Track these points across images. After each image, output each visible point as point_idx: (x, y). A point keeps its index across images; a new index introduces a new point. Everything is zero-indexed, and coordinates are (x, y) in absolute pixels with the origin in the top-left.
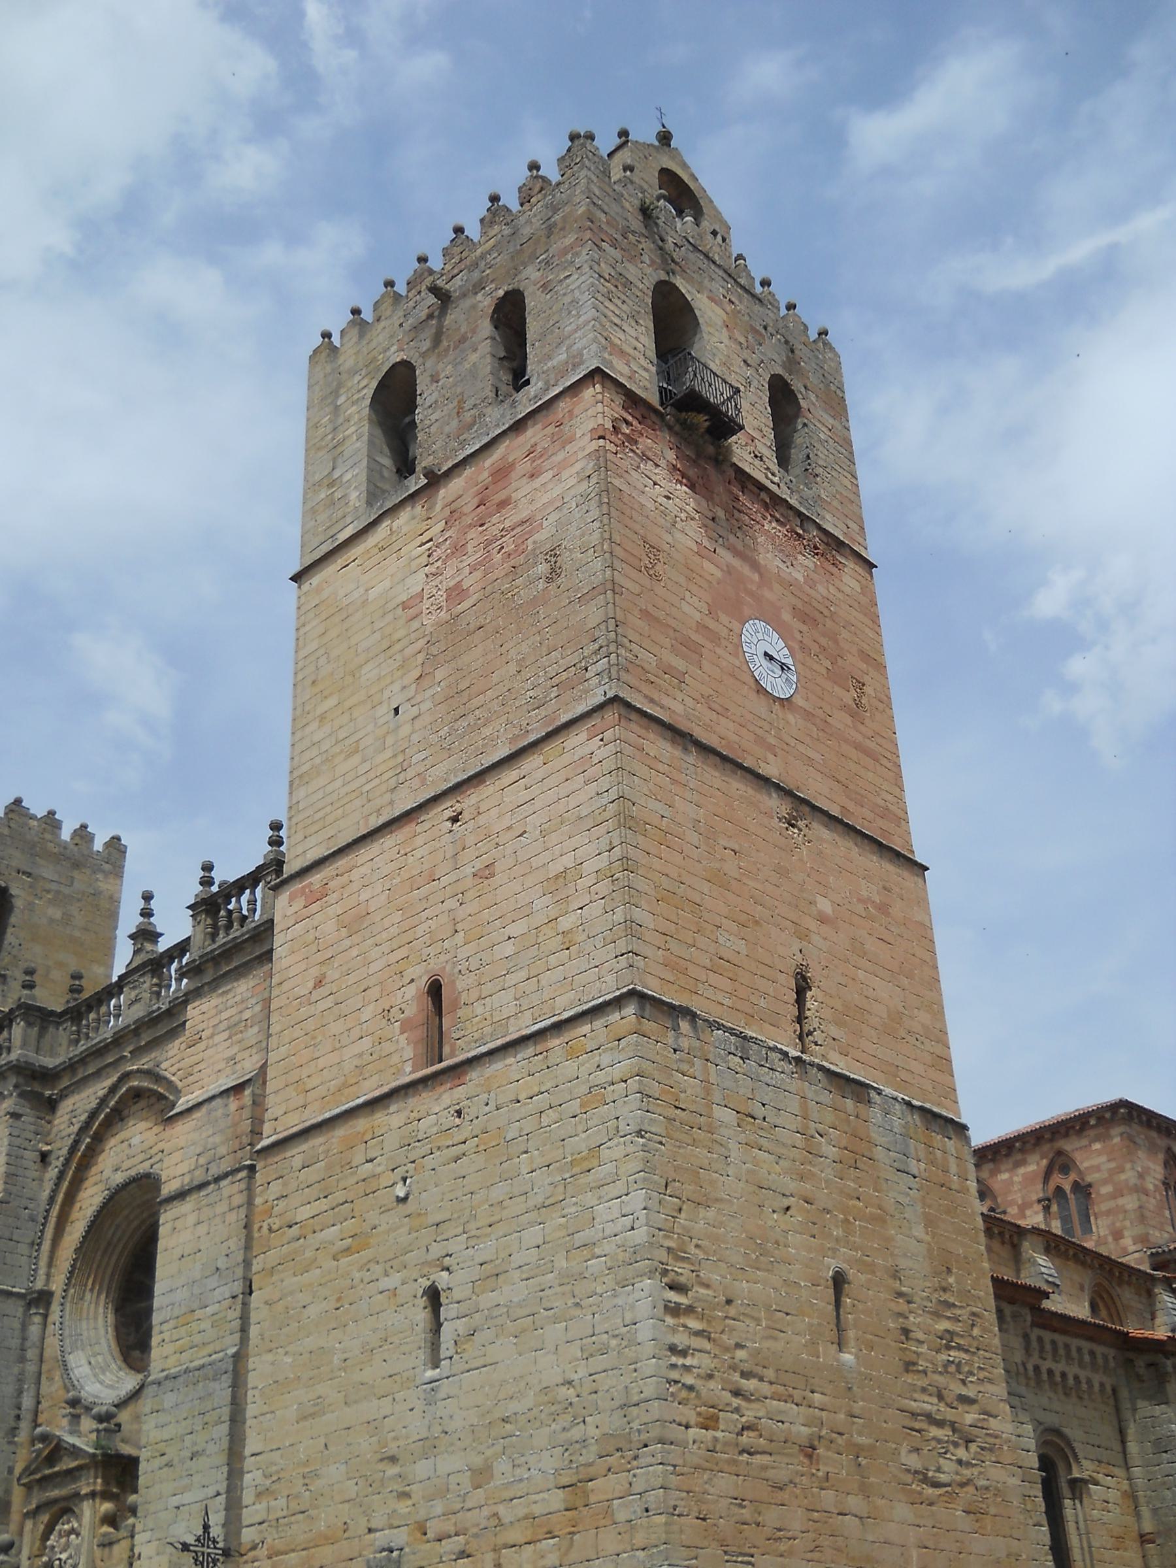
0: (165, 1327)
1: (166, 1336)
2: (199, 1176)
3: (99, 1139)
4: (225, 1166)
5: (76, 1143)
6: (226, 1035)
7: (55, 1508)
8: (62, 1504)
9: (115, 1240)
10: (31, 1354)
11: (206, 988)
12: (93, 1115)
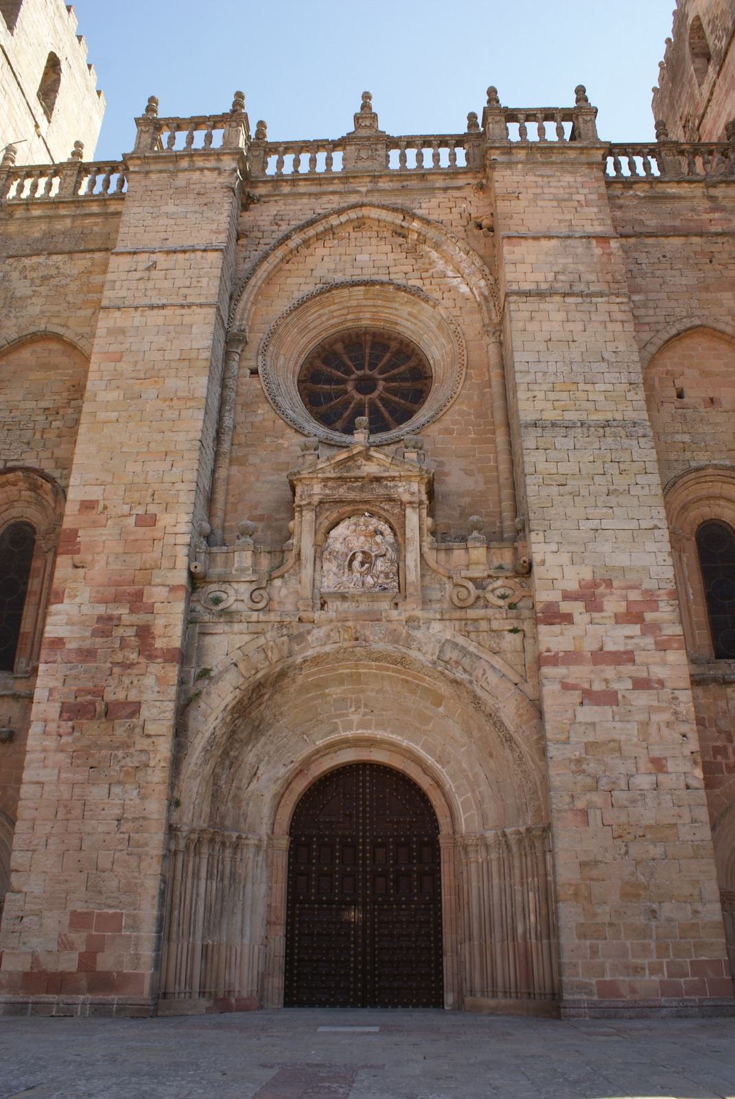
0: (535, 387)
1: (540, 395)
3: (306, 243)
4: (593, 288)
5: (287, 237)
6: (555, 204)
9: (312, 326)
10: (231, 382)
11: (520, 166)
12: (311, 223)
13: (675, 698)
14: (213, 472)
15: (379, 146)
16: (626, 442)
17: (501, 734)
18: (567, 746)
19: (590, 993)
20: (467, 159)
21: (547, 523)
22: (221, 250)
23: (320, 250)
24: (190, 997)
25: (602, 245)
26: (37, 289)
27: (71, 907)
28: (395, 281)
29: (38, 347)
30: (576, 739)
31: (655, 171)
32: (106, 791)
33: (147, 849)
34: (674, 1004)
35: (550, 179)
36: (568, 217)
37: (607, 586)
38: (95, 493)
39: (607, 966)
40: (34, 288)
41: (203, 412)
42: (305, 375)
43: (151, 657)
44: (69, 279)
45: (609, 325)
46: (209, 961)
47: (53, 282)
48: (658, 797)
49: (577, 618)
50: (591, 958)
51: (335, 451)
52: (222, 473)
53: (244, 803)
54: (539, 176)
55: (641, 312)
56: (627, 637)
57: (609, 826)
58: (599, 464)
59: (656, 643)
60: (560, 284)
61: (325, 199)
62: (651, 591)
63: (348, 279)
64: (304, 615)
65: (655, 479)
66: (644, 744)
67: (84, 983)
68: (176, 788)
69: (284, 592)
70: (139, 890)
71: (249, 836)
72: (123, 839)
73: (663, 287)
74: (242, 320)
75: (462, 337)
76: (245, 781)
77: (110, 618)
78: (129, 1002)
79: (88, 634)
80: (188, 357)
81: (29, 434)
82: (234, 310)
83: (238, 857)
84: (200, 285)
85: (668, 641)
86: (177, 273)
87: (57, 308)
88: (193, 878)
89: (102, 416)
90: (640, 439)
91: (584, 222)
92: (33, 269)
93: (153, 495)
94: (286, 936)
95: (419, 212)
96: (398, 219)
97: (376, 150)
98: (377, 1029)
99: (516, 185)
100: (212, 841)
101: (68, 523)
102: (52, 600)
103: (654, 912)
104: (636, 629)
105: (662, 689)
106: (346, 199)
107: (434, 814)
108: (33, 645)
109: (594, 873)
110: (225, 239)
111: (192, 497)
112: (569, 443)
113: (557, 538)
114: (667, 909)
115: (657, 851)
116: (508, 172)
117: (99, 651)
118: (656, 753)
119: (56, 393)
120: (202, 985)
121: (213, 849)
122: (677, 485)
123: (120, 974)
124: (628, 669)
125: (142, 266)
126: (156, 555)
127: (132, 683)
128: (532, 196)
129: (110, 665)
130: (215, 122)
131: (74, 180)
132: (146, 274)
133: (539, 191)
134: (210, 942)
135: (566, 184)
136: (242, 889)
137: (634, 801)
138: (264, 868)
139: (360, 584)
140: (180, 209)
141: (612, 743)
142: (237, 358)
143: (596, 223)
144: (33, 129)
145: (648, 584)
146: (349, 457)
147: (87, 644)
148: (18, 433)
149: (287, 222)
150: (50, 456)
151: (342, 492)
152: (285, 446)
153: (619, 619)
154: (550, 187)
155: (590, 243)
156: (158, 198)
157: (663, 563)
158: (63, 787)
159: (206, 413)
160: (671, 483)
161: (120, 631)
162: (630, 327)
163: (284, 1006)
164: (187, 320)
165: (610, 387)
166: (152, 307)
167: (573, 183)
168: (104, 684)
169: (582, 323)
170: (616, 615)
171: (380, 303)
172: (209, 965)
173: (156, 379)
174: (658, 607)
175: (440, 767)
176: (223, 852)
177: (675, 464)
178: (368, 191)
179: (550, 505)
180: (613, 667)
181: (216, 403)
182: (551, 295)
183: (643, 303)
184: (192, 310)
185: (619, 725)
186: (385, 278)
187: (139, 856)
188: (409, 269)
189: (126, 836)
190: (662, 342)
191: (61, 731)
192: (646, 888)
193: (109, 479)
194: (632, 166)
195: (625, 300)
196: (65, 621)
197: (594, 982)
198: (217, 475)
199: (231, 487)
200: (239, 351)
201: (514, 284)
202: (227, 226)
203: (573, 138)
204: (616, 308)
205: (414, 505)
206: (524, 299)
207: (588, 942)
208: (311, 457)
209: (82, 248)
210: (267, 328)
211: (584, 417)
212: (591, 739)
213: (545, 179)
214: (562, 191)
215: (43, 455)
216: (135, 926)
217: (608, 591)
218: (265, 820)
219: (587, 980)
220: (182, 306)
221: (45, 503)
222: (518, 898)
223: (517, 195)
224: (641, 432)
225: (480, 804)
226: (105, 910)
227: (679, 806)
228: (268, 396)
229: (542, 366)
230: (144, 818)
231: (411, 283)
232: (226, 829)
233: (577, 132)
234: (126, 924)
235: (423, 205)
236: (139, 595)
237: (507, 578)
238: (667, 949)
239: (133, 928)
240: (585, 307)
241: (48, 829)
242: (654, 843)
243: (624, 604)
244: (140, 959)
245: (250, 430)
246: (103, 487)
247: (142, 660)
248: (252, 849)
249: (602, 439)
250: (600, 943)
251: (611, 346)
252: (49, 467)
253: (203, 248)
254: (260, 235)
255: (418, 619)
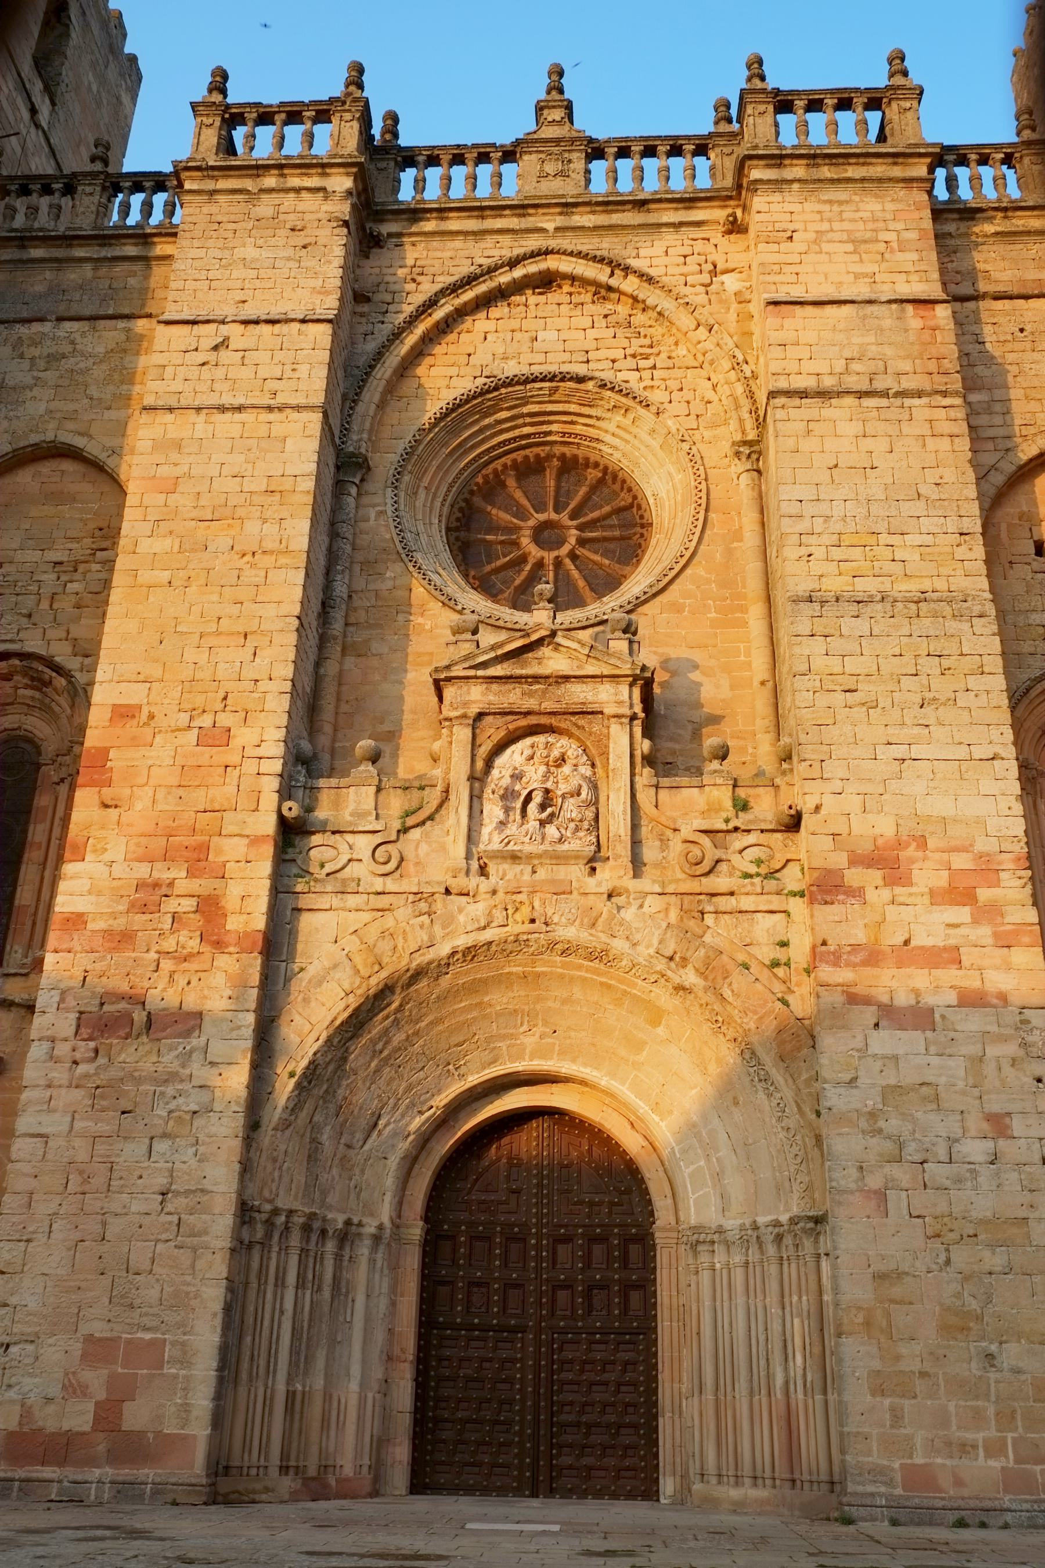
0: (813, 540)
1: (819, 553)
2: (853, 382)
3: (461, 313)
4: (908, 383)
5: (432, 303)
6: (850, 247)
7: (523, 722)
8: (544, 720)
10: (345, 529)
11: (796, 186)
12: (469, 281)
13: (1028, 1022)
14: (318, 665)
15: (574, 156)
16: (952, 626)
17: (752, 1070)
18: (855, 1091)
19: (890, 1483)
20: (713, 176)
21: (825, 748)
22: (329, 321)
23: (480, 323)
24: (266, 1474)
25: (922, 313)
26: (41, 375)
27: (84, 1329)
28: (597, 374)
29: (46, 468)
30: (869, 1081)
31: (1013, 192)
32: (144, 1148)
33: (205, 1238)
34: (1025, 1506)
35: (843, 208)
36: (873, 268)
37: (918, 847)
38: (134, 694)
39: (919, 1441)
40: (35, 374)
41: (302, 573)
42: (458, 520)
43: (219, 945)
44: (91, 360)
45: (929, 441)
46: (297, 1416)
47: (69, 363)
48: (997, 1174)
49: (871, 895)
50: (892, 1426)
51: (503, 636)
52: (331, 668)
53: (357, 1171)
54: (825, 202)
55: (983, 420)
56: (949, 925)
57: (918, 1217)
58: (908, 658)
59: (996, 935)
60: (855, 378)
61: (490, 241)
62: (988, 855)
63: (525, 370)
64: (454, 884)
65: (999, 682)
66: (976, 1092)
67: (101, 1448)
68: (254, 1145)
69: (424, 848)
70: (193, 1303)
71: (365, 1220)
72: (170, 1223)
73: (1018, 379)
74: (361, 432)
75: (699, 462)
76: (359, 1136)
77: (156, 885)
78: (173, 1480)
79: (122, 907)
80: (281, 488)
81: (30, 601)
82: (350, 416)
83: (347, 1253)
84: (296, 375)
85: (1016, 933)
86: (263, 357)
87: (71, 407)
88: (276, 1285)
89: (146, 576)
90: (975, 621)
91: (896, 277)
92: (34, 343)
93: (225, 698)
94: (416, 1380)
95: (634, 263)
96: (601, 273)
97: (570, 161)
98: (556, 1528)
99: (788, 217)
100: (307, 1228)
101: (92, 739)
102: (67, 855)
103: (990, 1356)
104: (963, 914)
105: (1005, 1007)
106: (524, 243)
107: (646, 1191)
108: (34, 924)
109: (897, 1291)
110: (336, 304)
111: (285, 702)
112: (862, 626)
113: (842, 773)
114: (1012, 1354)
115: (996, 1260)
116: (777, 197)
117: (140, 934)
118: (995, 1106)
119: (72, 539)
120: (285, 1455)
121: (308, 1241)
122: (1033, 693)
123: (158, 1434)
124: (949, 976)
125: (207, 343)
126: (232, 789)
127: (189, 983)
128: (813, 235)
129: (156, 956)
130: (323, 113)
131: (96, 201)
132: (212, 357)
133: (825, 226)
134: (299, 1387)
135: (869, 214)
136: (350, 1304)
137: (959, 1180)
138: (386, 1271)
139: (539, 838)
140: (265, 253)
141: (924, 1089)
142: (354, 491)
143: (914, 277)
144: (26, 115)
145: (982, 845)
146: (524, 646)
147: (120, 924)
148: (14, 599)
149: (430, 278)
150: (64, 635)
151: (514, 697)
152: (427, 627)
153: (938, 897)
154: (842, 220)
155: (903, 310)
156: (230, 235)
157: (1008, 813)
158: (77, 1142)
159: (307, 575)
160: (1022, 689)
161: (171, 905)
162: (964, 444)
163: (411, 1493)
164: (277, 430)
165: (929, 540)
166: (222, 409)
167: (879, 214)
168: (146, 984)
169: (888, 439)
170: (932, 893)
171: (573, 408)
172: (296, 1425)
173: (230, 521)
174: (999, 880)
175: (657, 1119)
176: (323, 1245)
177: (1030, 660)
178: (557, 229)
179: (830, 721)
180: (926, 971)
181: (323, 562)
182: (839, 394)
183: (985, 406)
184: (284, 414)
185: (935, 1061)
186: (581, 370)
187: (194, 1250)
188: (619, 354)
189: (175, 1219)
190: (1014, 468)
191: (78, 1056)
192: (979, 1318)
193: (157, 673)
194: (975, 182)
195: (958, 401)
196: (88, 887)
197: (896, 1465)
198: (322, 671)
199: (344, 688)
200: (357, 481)
201: (782, 378)
202: (338, 282)
203: (882, 138)
204: (942, 413)
205: (623, 720)
206: (797, 401)
207: (887, 1402)
208: (467, 645)
209: (110, 312)
210: (401, 446)
211: (887, 586)
212: (893, 1081)
213: (836, 208)
214: (861, 226)
215: (52, 634)
216: (185, 1361)
217: (920, 854)
218: (388, 1198)
219: (885, 1463)
220: (270, 409)
221: (57, 709)
222: (776, 1326)
223: (789, 234)
224: (977, 609)
225: (718, 1177)
226: (139, 1335)
227: (1031, 1191)
228: (401, 551)
229: (823, 508)
230: (202, 1191)
231: (621, 376)
232: (330, 1208)
233: (887, 129)
234: (170, 1357)
235: (643, 252)
236: (204, 849)
237: (762, 831)
238: (1013, 1418)
239: (182, 1363)
240: (893, 414)
241: (53, 1207)
242: (992, 1246)
243: (945, 874)
244: (189, 1411)
245: (373, 602)
246: (148, 685)
247: (206, 948)
248: (368, 1242)
249: (915, 621)
250: (907, 1403)
251: (932, 476)
252: (62, 654)
253: (301, 317)
254: (388, 298)
255: (627, 891)
